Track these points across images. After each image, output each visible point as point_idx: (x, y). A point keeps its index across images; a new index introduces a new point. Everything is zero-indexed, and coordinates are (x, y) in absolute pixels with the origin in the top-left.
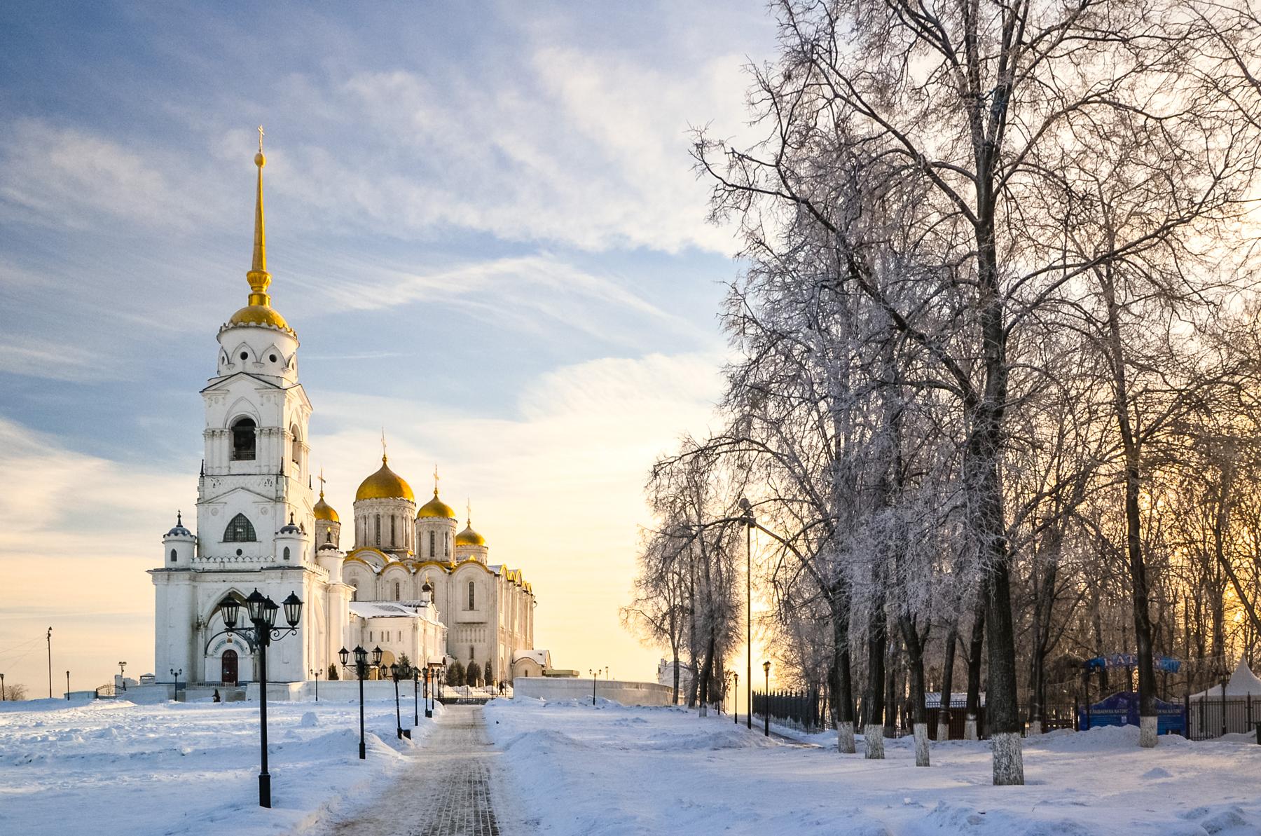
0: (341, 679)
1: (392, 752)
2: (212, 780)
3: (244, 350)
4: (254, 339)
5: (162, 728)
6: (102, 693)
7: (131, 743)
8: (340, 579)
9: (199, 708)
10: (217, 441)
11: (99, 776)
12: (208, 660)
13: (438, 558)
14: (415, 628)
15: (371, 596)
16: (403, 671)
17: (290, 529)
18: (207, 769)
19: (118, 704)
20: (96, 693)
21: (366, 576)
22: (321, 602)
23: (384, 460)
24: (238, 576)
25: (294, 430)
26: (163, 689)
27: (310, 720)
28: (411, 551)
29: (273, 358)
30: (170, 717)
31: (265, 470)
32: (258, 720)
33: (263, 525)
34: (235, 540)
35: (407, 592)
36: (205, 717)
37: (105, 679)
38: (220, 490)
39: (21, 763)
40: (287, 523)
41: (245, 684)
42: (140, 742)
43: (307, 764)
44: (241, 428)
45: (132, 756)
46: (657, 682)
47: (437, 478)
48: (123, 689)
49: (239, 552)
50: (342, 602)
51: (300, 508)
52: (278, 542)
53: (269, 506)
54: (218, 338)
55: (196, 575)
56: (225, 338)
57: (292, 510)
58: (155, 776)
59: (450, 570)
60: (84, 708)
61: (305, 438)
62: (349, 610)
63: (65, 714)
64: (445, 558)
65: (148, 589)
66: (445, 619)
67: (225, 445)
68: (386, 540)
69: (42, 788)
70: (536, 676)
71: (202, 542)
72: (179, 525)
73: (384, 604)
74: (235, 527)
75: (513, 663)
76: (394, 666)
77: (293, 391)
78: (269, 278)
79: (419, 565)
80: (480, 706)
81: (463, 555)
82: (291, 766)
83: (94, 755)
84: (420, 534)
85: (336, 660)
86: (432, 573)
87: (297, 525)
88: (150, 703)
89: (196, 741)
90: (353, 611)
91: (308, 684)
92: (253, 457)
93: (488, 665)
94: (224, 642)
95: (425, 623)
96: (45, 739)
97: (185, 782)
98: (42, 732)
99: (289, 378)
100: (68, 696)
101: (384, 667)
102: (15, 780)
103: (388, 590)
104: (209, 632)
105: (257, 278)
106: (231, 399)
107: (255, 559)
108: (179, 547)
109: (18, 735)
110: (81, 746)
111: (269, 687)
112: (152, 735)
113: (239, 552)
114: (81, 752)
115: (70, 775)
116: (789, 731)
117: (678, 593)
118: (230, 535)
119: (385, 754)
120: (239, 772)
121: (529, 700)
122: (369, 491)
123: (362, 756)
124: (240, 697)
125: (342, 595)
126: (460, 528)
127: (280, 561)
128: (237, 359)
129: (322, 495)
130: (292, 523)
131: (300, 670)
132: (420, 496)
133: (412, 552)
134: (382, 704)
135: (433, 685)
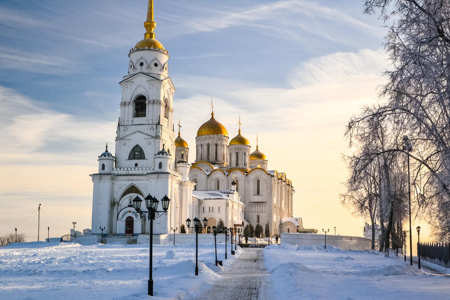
0: (187, 233)
1: (212, 272)
2: (123, 285)
3: (141, 61)
4: (147, 55)
5: (95, 258)
6: (64, 239)
7: (81, 265)
8: (188, 179)
9: (114, 247)
10: (127, 108)
11: (69, 281)
12: (119, 222)
13: (241, 166)
14: (227, 205)
15: (204, 187)
16: (220, 229)
17: (163, 152)
18: (120, 279)
19: (73, 245)
20: (62, 239)
21: (202, 177)
22: (178, 191)
23: (212, 114)
24: (135, 178)
25: (166, 101)
26: (96, 237)
27: (170, 255)
28: (225, 163)
29: (156, 65)
30: (98, 252)
31: (150, 122)
32: (148, 254)
33: (149, 151)
34: (134, 158)
35: (223, 186)
36: (117, 253)
37: (65, 232)
38: (127, 133)
39: (31, 274)
40: (161, 149)
41: (137, 235)
42: (86, 265)
43: (169, 277)
44: (139, 101)
45: (84, 272)
46: (363, 236)
47: (240, 124)
48: (75, 237)
49: (136, 165)
50: (189, 190)
51: (168, 141)
52: (157, 159)
53: (152, 141)
54: (129, 55)
55: (114, 177)
56: (132, 55)
57: (164, 143)
58: (96, 282)
59: (247, 173)
60: (56, 247)
61: (172, 105)
62: (192, 195)
63: (47, 250)
64: (244, 167)
65: (90, 184)
66: (243, 200)
67: (131, 109)
68: (212, 157)
69: (43, 286)
70: (293, 232)
71: (118, 160)
72: (107, 151)
73: (211, 192)
74: (135, 152)
75: (281, 225)
76: (214, 227)
77: (166, 81)
78: (155, 24)
79: (230, 170)
80: (262, 249)
81: (254, 165)
82: (161, 278)
83: (65, 271)
84: (230, 154)
85: (185, 224)
86: (237, 175)
87: (166, 150)
88: (88, 245)
89: (113, 265)
90: (195, 196)
91: (170, 235)
92: (145, 115)
93: (267, 226)
94: (127, 213)
95: (233, 202)
96: (39, 263)
97: (110, 285)
98: (37, 259)
99: (164, 74)
100: (48, 240)
101: (209, 228)
102: (30, 282)
103: (213, 184)
104: (119, 207)
105: (149, 25)
106: (134, 86)
107: (144, 169)
108: (107, 163)
109: (25, 260)
110: (57, 266)
111: (153, 237)
112: (91, 262)
113: (136, 165)
114: (57, 269)
115: (55, 280)
116: (436, 266)
117: (373, 186)
118: (132, 155)
119: (209, 274)
120: (136, 281)
121: (289, 246)
122: (204, 131)
123: (197, 274)
124: (134, 242)
125: (189, 187)
126: (252, 150)
127: (157, 169)
128: (138, 66)
129: (179, 134)
130: (163, 149)
131: (166, 228)
132: (231, 134)
133: (226, 164)
134: (209, 246)
135: (236, 237)
